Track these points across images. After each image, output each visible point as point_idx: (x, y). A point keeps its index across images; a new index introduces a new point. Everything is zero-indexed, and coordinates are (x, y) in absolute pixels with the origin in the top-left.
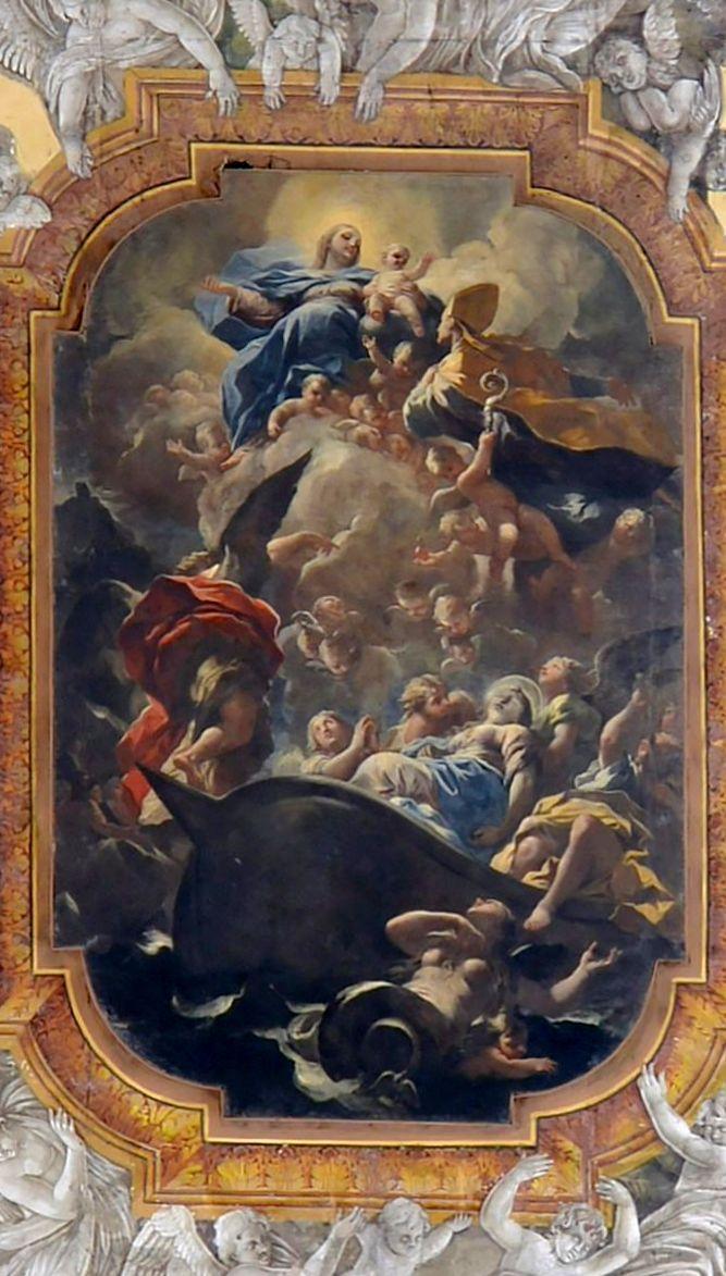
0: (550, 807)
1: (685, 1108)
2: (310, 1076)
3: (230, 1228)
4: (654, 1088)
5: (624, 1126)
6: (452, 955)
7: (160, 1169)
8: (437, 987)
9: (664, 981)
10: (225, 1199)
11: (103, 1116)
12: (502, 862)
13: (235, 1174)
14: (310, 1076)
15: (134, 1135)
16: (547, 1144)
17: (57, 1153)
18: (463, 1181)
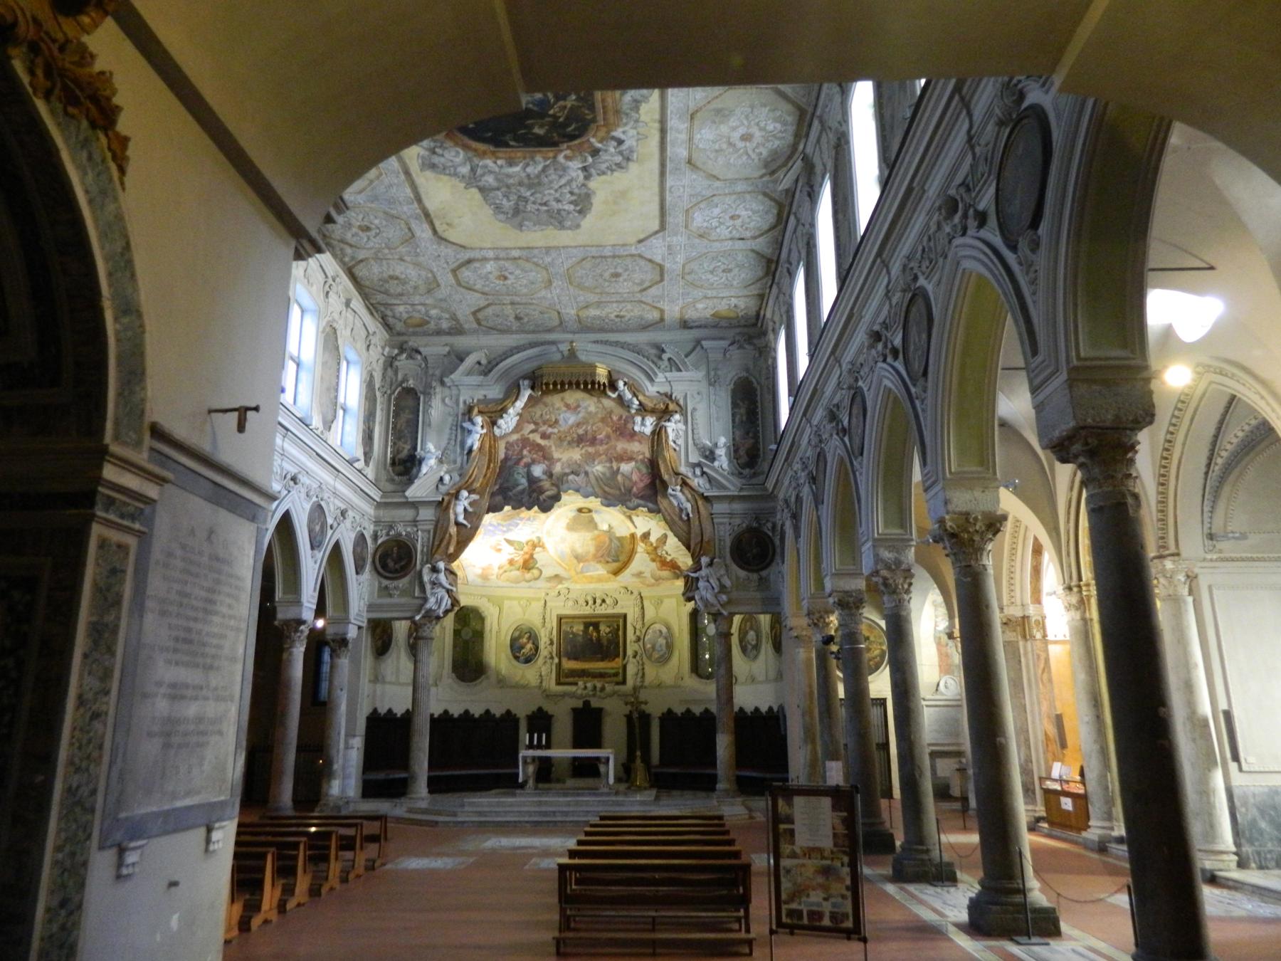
0: (561, 103)
1: (601, 142)
2: (512, 143)
3: (499, 162)
4: (593, 140)
5: (586, 146)
6: (541, 126)
7: (483, 155)
8: (538, 131)
9: (593, 126)
10: (498, 158)
11: (465, 147)
12: (551, 112)
13: (500, 155)
14: (512, 143)
15: (475, 150)
16: (568, 148)
17: (458, 153)
18: (551, 155)
